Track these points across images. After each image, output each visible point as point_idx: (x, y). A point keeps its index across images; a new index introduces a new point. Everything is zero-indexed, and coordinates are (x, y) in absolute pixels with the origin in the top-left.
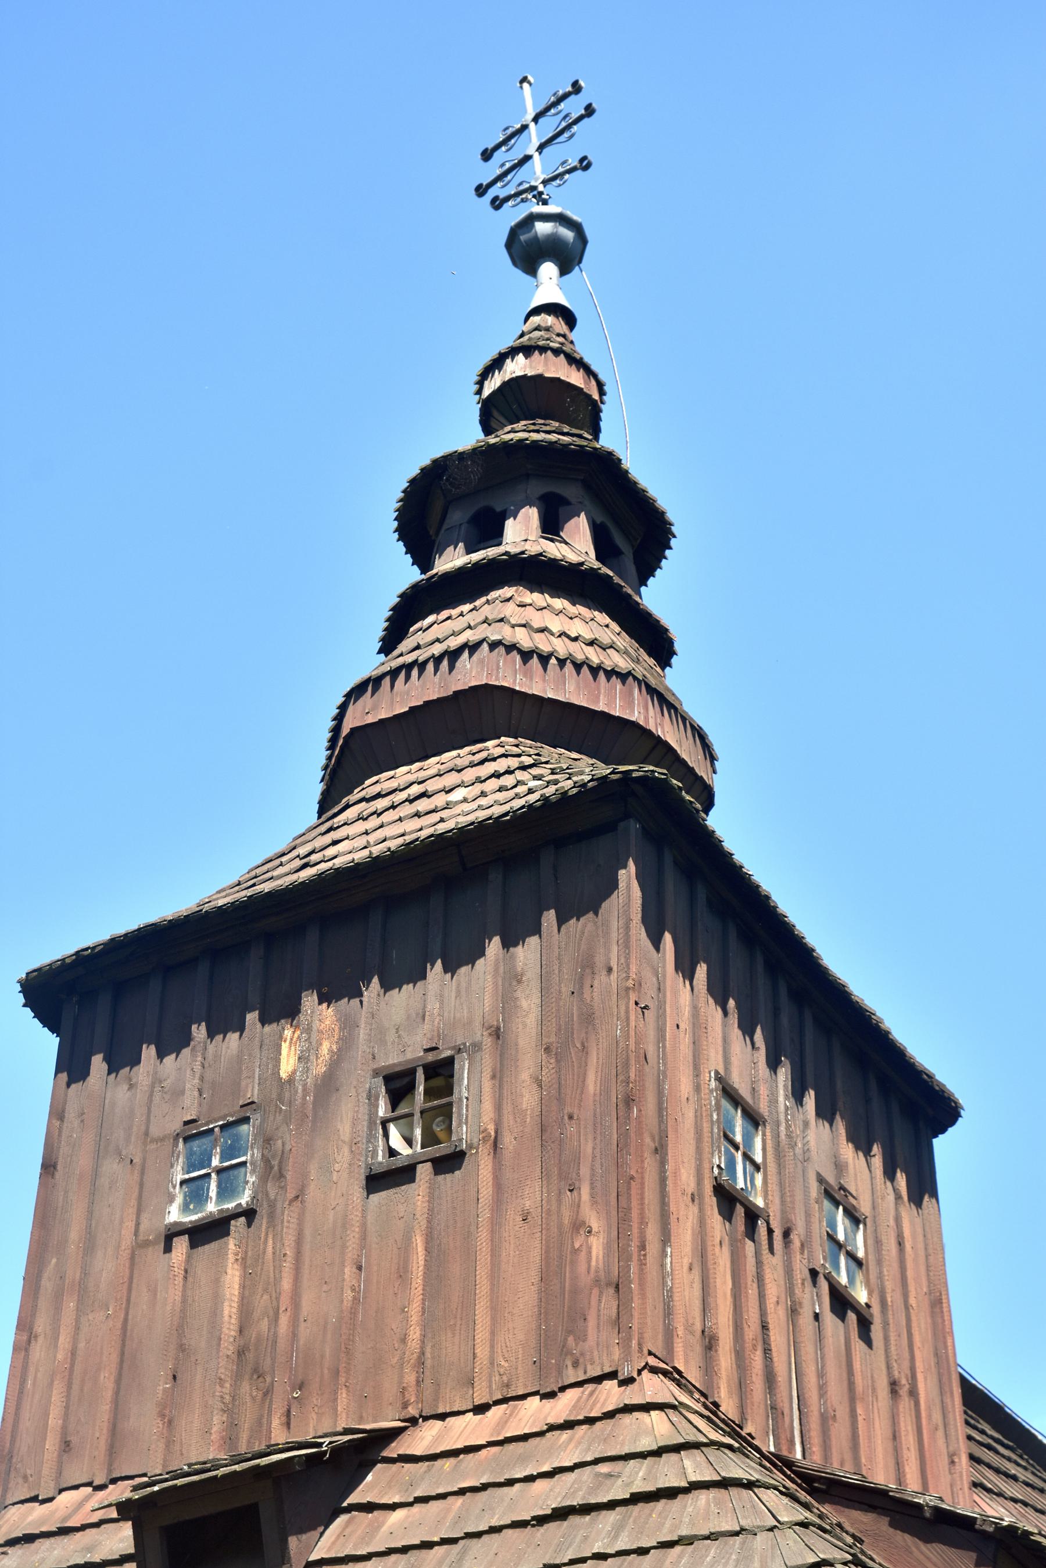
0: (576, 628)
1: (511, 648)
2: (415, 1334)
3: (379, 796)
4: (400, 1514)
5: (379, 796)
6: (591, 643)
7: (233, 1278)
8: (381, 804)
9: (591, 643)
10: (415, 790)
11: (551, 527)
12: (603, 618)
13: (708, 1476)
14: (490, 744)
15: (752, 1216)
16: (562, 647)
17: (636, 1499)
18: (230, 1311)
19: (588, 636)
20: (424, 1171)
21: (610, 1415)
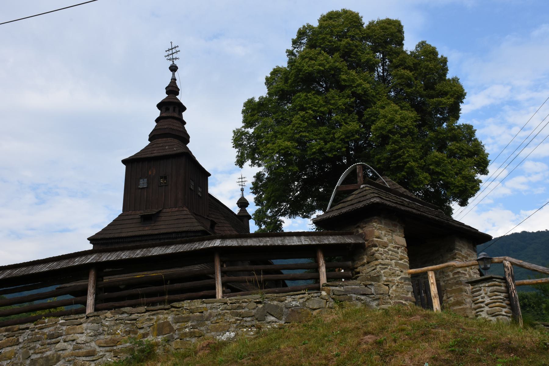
0: (177, 125)
1: (171, 128)
2: (163, 201)
3: (157, 144)
4: (163, 217)
5: (157, 144)
6: (179, 127)
7: (145, 193)
8: (158, 145)
9: (179, 127)
10: (161, 145)
11: (174, 111)
12: (180, 123)
13: (189, 217)
14: (169, 139)
15: (192, 190)
16: (175, 128)
17: (184, 218)
18: (145, 196)
19: (178, 126)
20: (164, 186)
21: (181, 211)
